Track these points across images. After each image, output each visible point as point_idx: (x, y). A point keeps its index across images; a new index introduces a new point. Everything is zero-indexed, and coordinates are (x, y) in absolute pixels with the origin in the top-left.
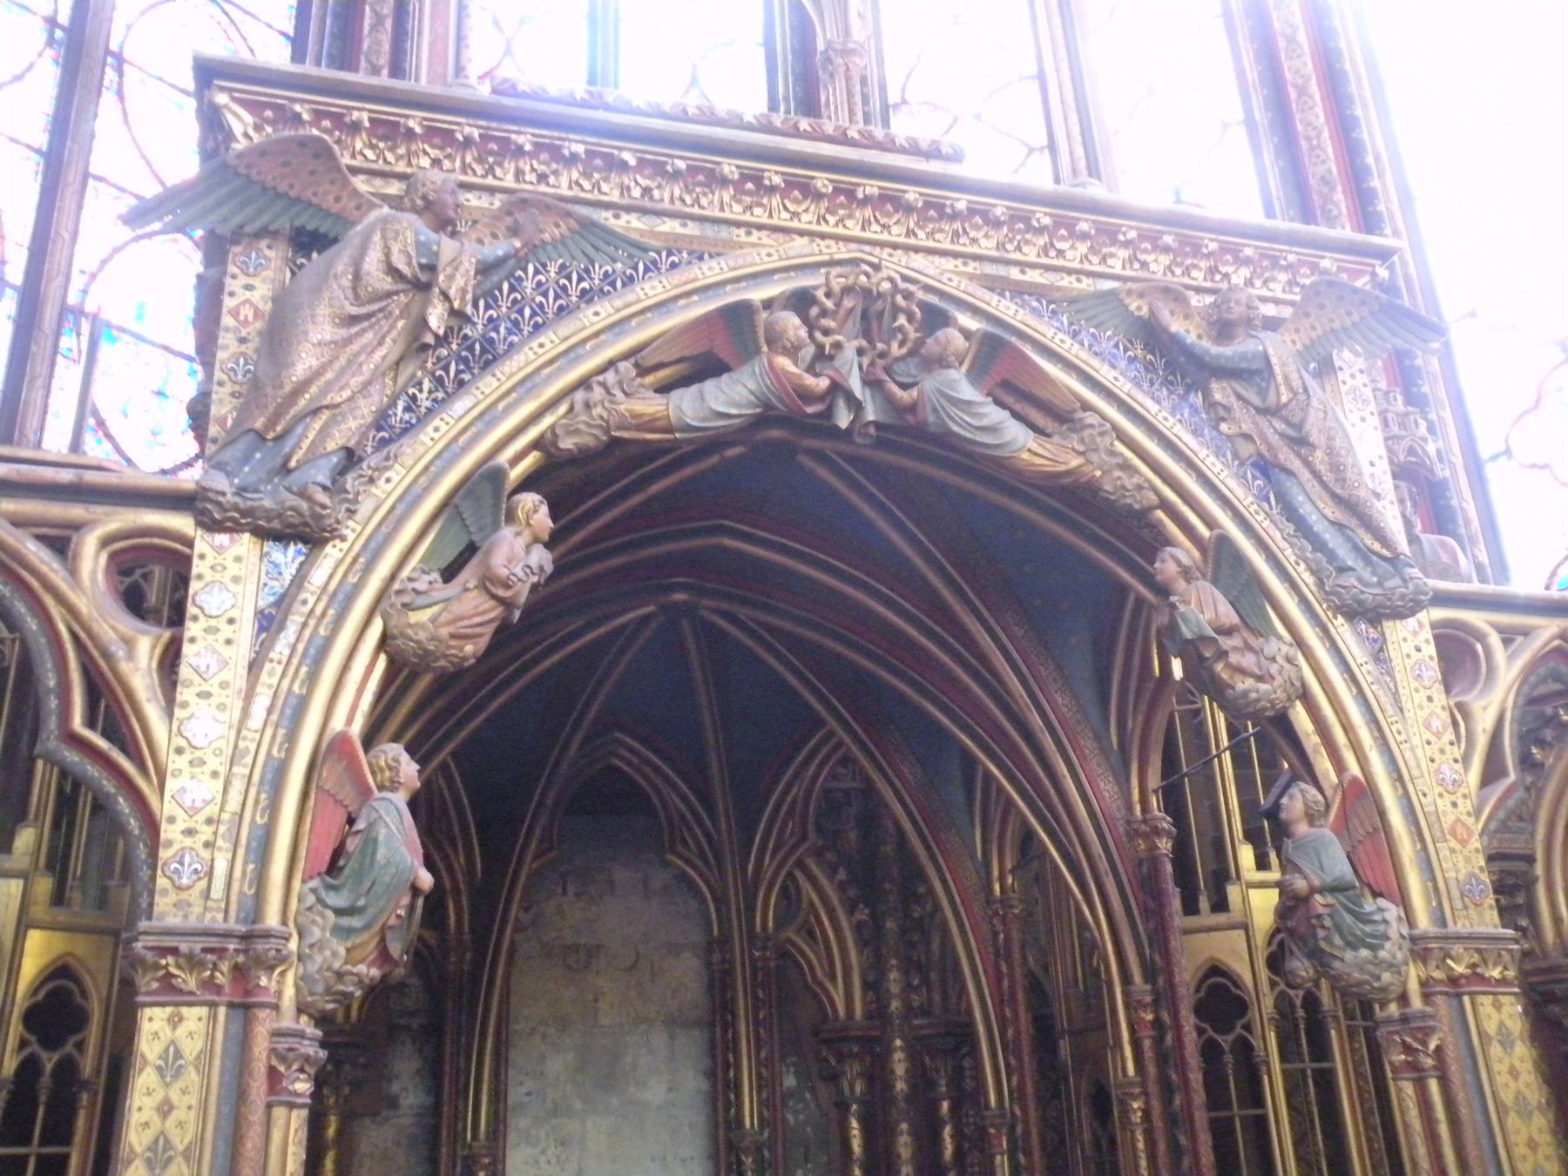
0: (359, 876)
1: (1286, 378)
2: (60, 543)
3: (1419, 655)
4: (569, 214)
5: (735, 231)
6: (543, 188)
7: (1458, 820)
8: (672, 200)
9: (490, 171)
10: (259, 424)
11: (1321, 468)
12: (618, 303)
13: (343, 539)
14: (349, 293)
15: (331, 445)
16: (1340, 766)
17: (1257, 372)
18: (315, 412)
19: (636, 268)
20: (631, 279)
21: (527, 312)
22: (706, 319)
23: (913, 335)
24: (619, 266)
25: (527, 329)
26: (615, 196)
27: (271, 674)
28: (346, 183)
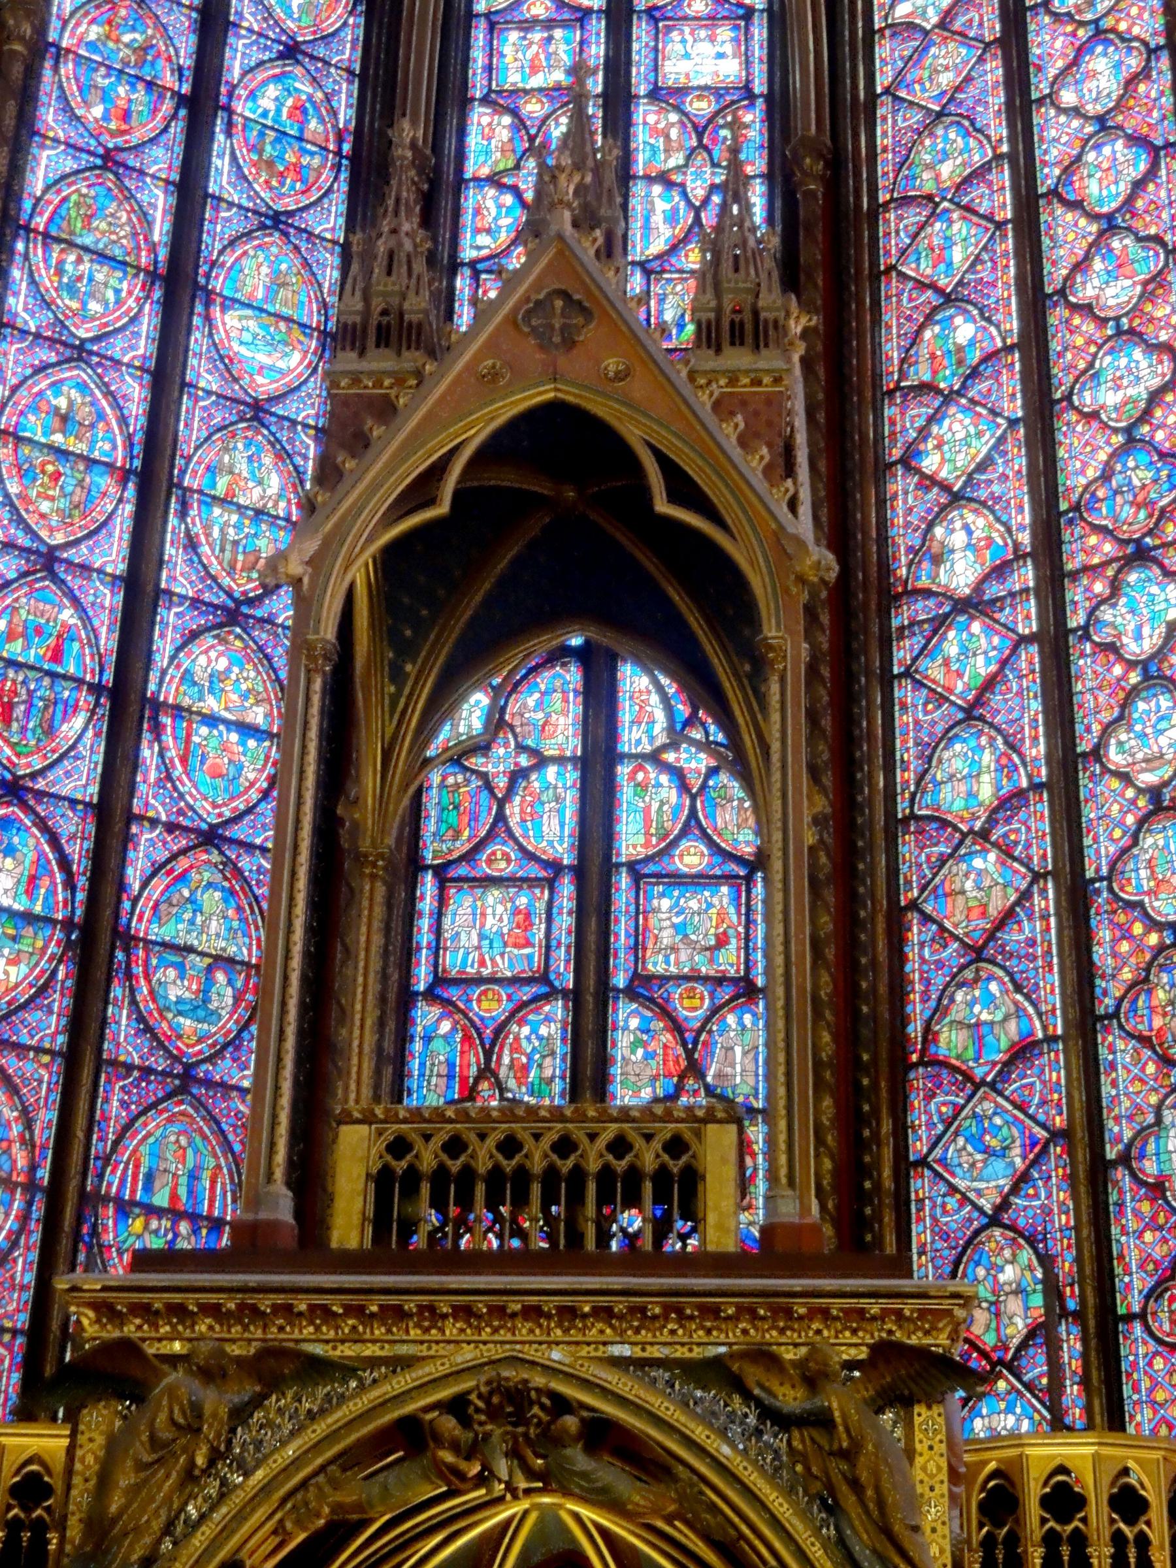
11: (871, 1505)
15: (134, 1557)
18: (126, 1534)
20: (342, 1399)
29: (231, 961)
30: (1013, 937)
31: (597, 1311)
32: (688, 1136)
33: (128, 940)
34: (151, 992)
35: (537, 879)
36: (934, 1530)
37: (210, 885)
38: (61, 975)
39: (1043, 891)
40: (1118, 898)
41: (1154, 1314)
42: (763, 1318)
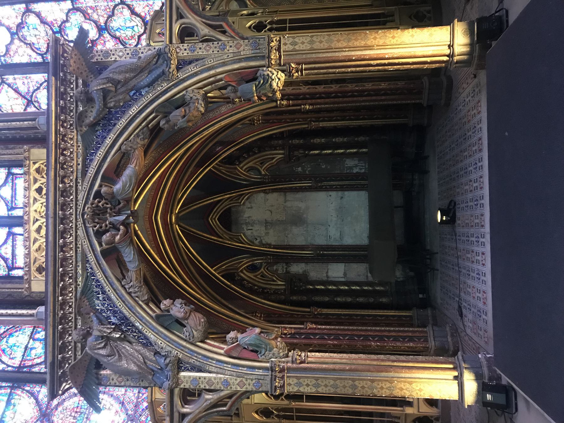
0: (258, 347)
1: (104, 84)
2: (183, 416)
4: (80, 299)
6: (73, 306)
7: (235, 46)
8: (72, 270)
10: (150, 377)
11: (132, 75)
12: (105, 285)
14: (112, 357)
15: (154, 359)
16: (221, 80)
18: (145, 362)
19: (94, 279)
20: (97, 280)
22: (106, 262)
23: (103, 201)
26: (73, 286)
28: (81, 359)
29: (32, 333)
30: (23, 89)
31: (63, 182)
32: (37, 166)
33: (20, 367)
34: (38, 358)
35: (13, 239)
36: (142, 53)
37: (7, 342)
38: (27, 388)
39: (7, 79)
40: (6, 54)
42: (66, 117)
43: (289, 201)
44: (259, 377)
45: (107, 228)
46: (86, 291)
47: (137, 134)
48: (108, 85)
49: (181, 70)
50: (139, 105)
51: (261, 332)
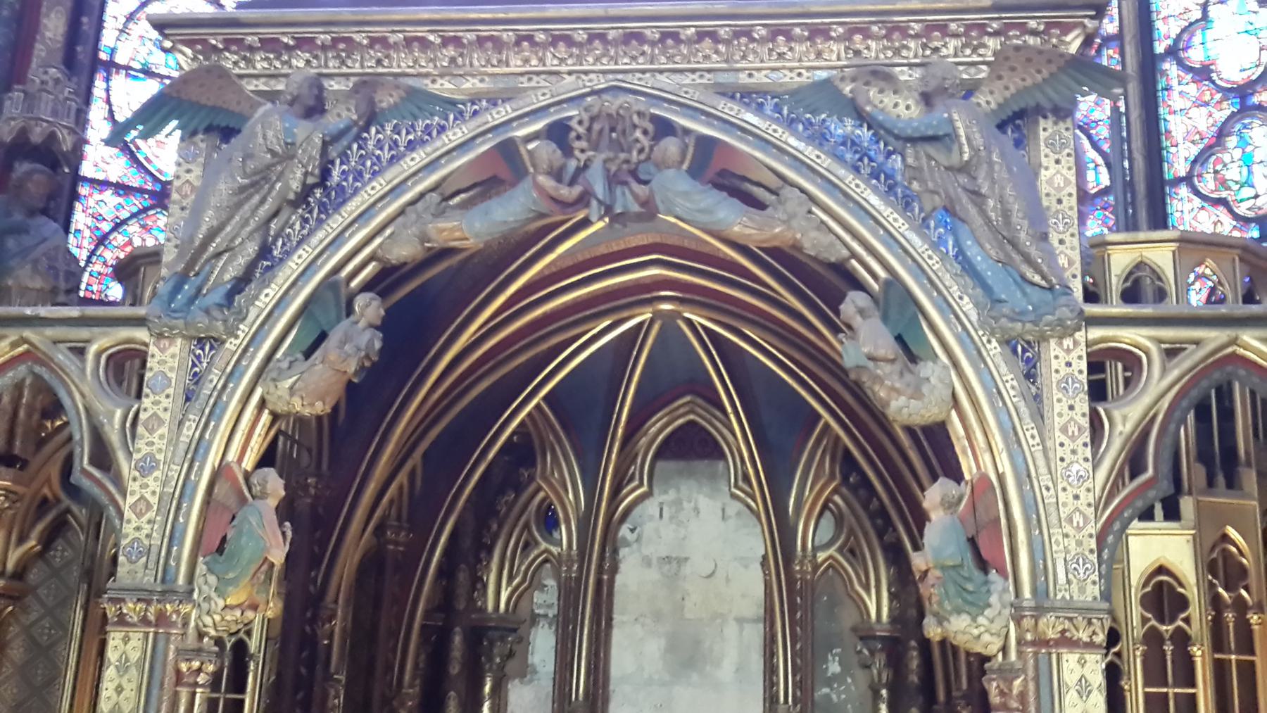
1: (968, 139)
2: (80, 352)
3: (1069, 370)
4: (397, 87)
5: (521, 79)
7: (1077, 509)
9: (343, 63)
11: (993, 215)
13: (237, 337)
15: (227, 277)
17: (947, 135)
18: (218, 255)
19: (447, 119)
20: (442, 129)
21: (369, 163)
24: (437, 118)
25: (367, 176)
27: (188, 429)
28: (241, 90)
41: (1200, 176)
43: (741, 630)
44: (153, 556)
45: (577, 153)
46: (419, 101)
47: (830, 230)
48: (966, 148)
49: (1008, 351)
50: (907, 234)
51: (272, 565)
